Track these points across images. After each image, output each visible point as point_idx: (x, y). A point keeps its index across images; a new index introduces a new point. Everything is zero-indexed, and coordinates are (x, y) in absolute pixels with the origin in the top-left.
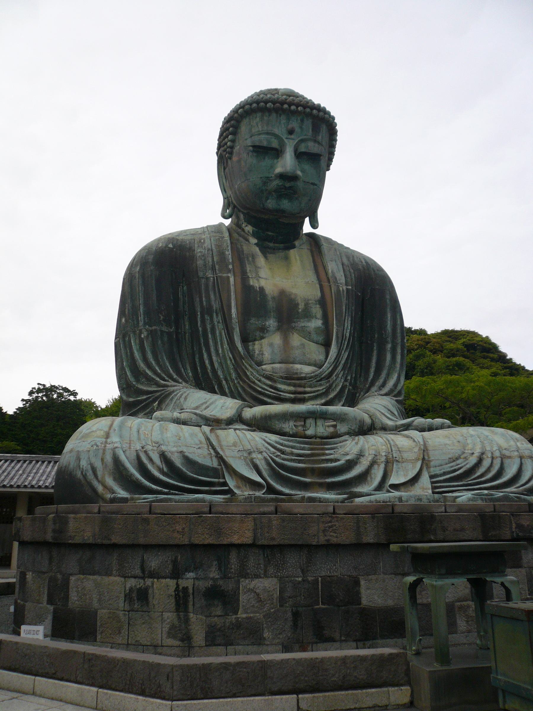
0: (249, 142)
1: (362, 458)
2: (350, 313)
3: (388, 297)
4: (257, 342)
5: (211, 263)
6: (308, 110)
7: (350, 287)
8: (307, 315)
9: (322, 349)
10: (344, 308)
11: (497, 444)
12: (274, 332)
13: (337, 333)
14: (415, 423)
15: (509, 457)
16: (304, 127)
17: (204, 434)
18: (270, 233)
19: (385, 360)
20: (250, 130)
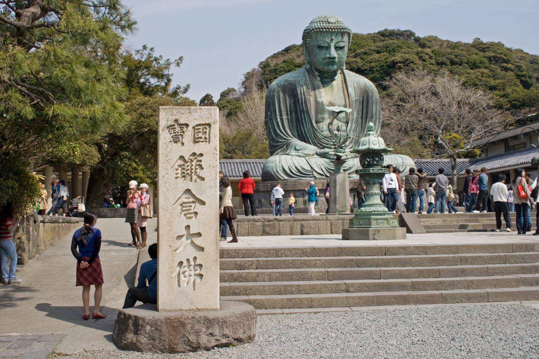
0: (316, 44)
5: (303, 92)
20: (316, 39)
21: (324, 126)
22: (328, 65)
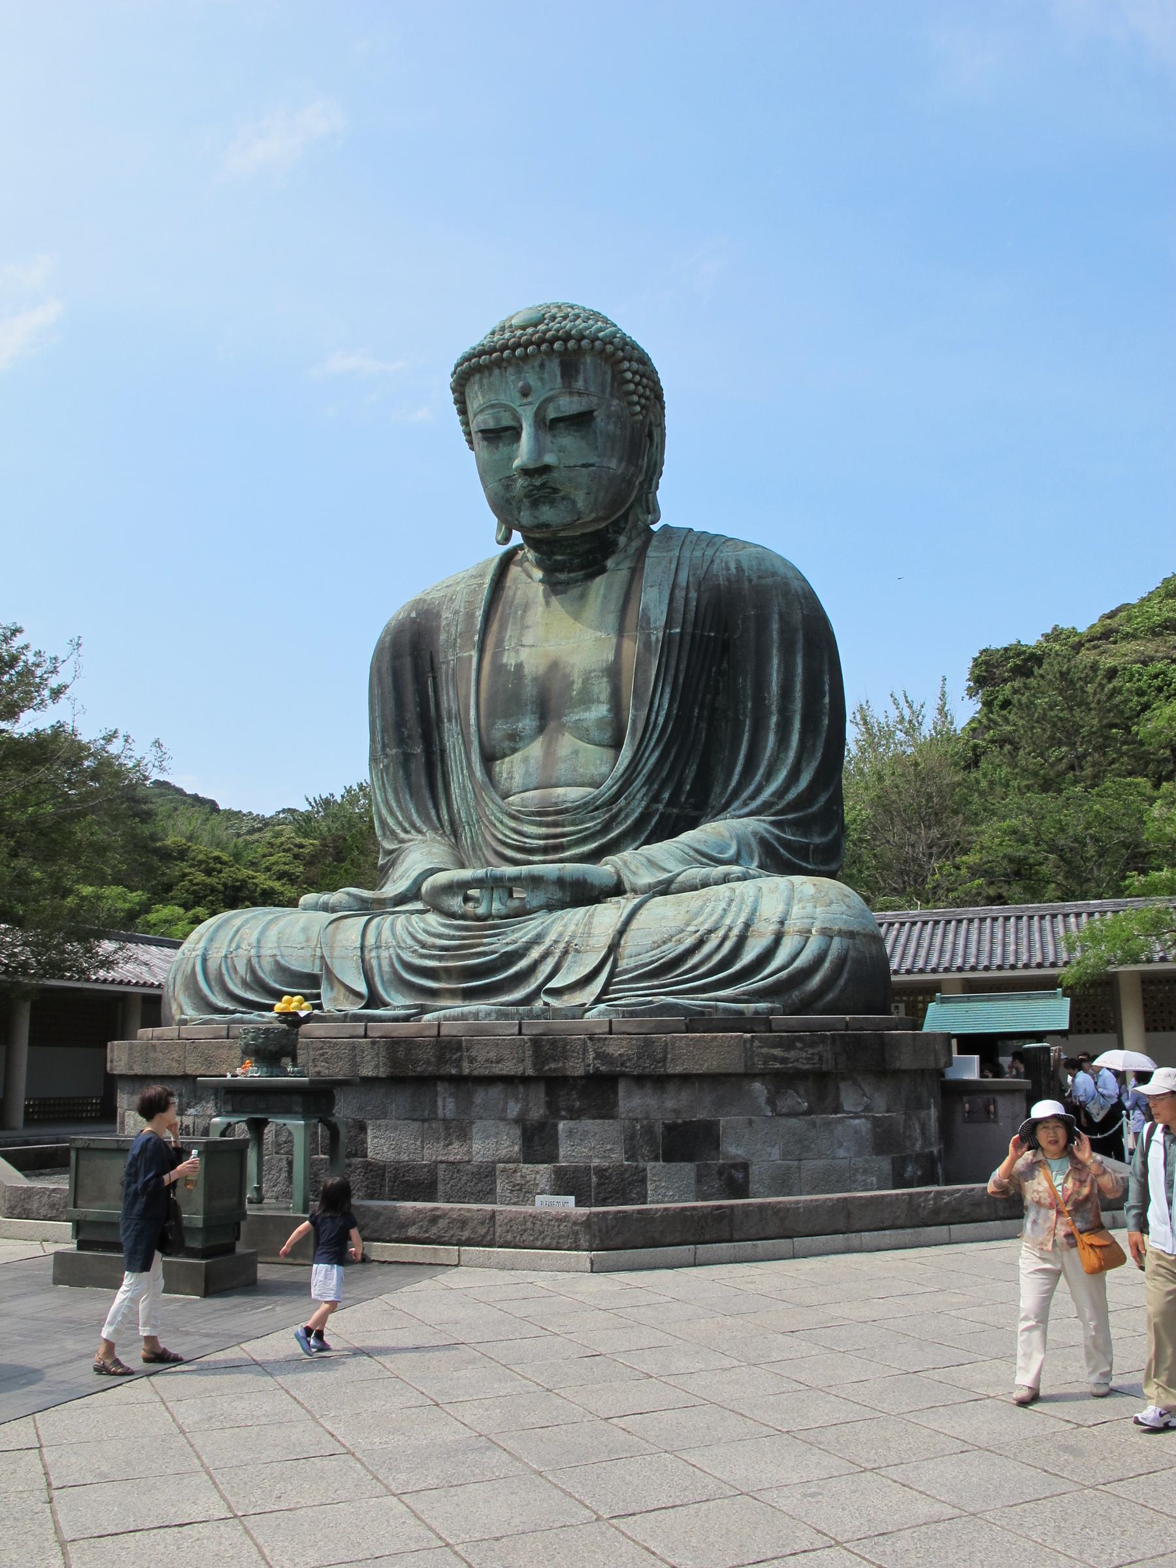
1: (536, 947)
2: (670, 679)
3: (775, 626)
4: (507, 759)
6: (544, 347)
7: (678, 630)
8: (586, 700)
9: (610, 753)
10: (654, 673)
11: (754, 911)
12: (533, 738)
14: (680, 878)
15: (761, 935)
16: (546, 376)
18: (559, 558)
19: (765, 747)
22: (535, 504)
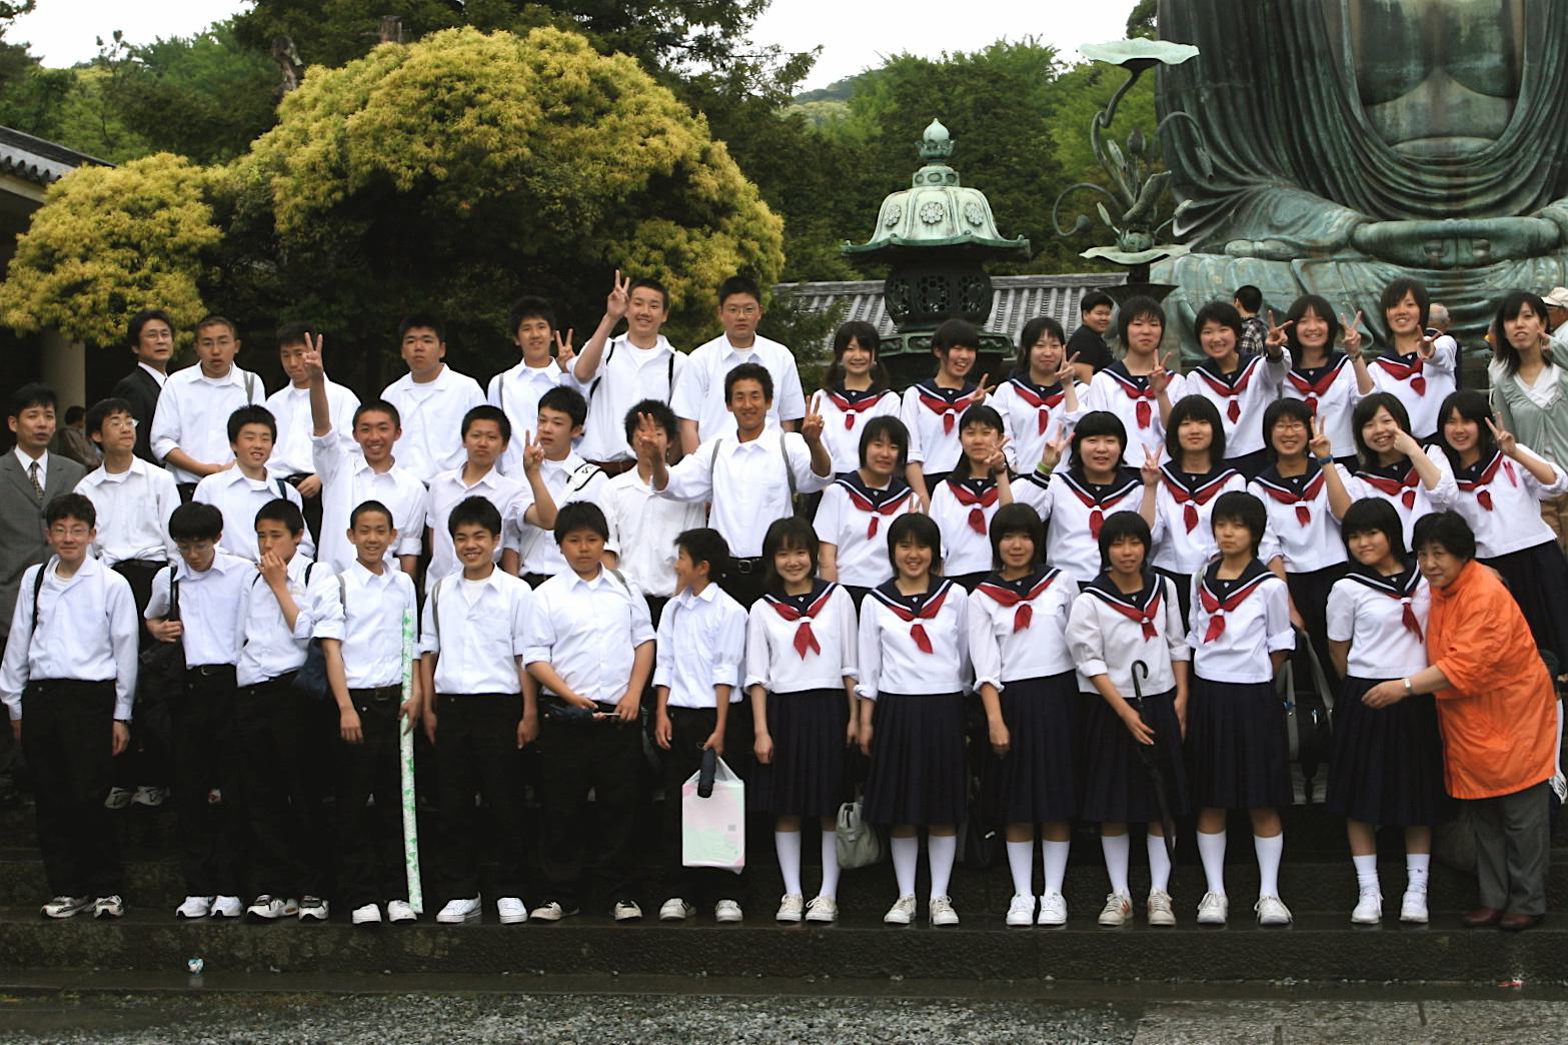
4: (1388, 104)
8: (1476, 48)
9: (1502, 105)
12: (1417, 84)
13: (1529, 74)
17: (1293, 273)
21: (1402, 113)
